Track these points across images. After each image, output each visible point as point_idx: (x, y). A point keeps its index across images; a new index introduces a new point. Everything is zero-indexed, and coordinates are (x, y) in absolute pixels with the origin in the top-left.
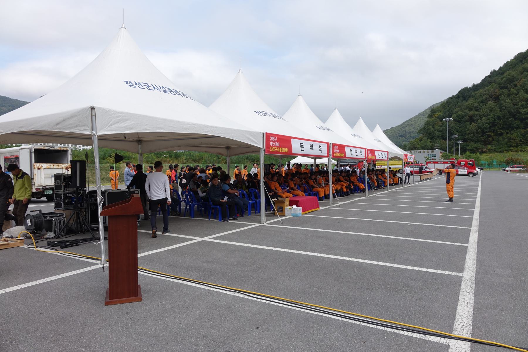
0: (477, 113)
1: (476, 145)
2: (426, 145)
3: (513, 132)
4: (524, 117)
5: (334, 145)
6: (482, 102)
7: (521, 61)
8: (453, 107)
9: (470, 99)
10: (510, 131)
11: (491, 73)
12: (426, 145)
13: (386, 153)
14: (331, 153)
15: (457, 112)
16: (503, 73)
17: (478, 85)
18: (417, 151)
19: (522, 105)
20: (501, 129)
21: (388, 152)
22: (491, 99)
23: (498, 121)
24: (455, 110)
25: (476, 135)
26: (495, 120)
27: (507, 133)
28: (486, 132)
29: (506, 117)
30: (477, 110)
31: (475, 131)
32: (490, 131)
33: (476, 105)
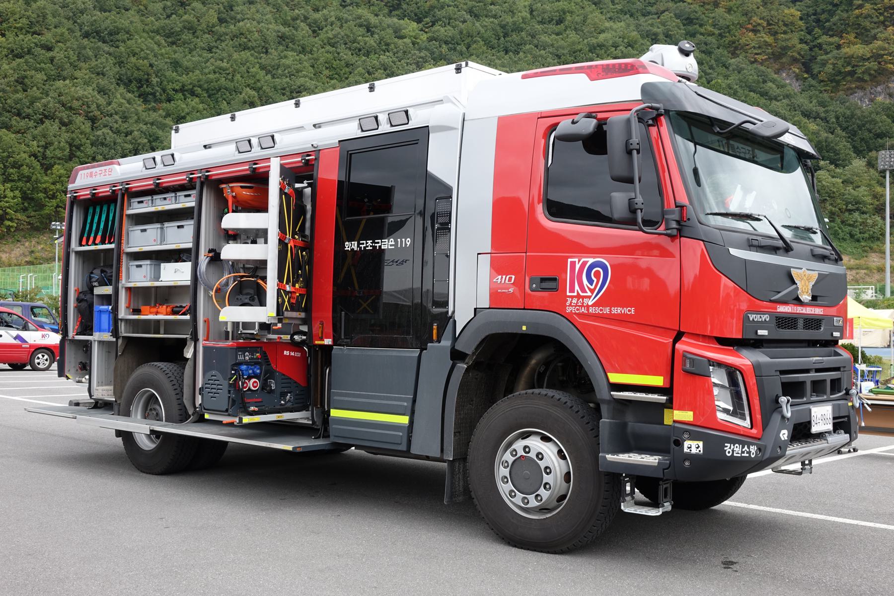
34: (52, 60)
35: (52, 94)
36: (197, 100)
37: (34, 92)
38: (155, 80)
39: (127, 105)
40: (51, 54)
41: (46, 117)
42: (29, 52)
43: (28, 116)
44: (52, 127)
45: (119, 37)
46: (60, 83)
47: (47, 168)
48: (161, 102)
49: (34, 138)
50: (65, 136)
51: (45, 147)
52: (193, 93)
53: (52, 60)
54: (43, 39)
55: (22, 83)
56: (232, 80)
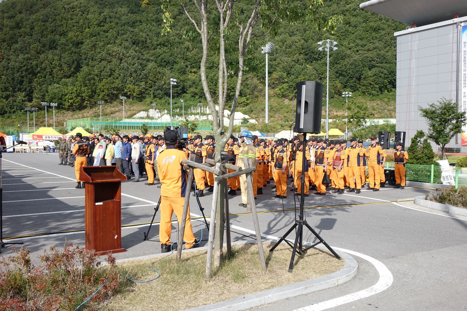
34: (107, 37)
35: (105, 50)
36: (165, 48)
37: (98, 50)
38: (148, 41)
40: (107, 34)
41: (103, 60)
42: (99, 34)
44: (104, 63)
45: (137, 24)
46: (109, 46)
47: (101, 80)
50: (109, 67)
51: (101, 72)
52: (164, 45)
53: (107, 37)
54: (104, 28)
56: (181, 39)
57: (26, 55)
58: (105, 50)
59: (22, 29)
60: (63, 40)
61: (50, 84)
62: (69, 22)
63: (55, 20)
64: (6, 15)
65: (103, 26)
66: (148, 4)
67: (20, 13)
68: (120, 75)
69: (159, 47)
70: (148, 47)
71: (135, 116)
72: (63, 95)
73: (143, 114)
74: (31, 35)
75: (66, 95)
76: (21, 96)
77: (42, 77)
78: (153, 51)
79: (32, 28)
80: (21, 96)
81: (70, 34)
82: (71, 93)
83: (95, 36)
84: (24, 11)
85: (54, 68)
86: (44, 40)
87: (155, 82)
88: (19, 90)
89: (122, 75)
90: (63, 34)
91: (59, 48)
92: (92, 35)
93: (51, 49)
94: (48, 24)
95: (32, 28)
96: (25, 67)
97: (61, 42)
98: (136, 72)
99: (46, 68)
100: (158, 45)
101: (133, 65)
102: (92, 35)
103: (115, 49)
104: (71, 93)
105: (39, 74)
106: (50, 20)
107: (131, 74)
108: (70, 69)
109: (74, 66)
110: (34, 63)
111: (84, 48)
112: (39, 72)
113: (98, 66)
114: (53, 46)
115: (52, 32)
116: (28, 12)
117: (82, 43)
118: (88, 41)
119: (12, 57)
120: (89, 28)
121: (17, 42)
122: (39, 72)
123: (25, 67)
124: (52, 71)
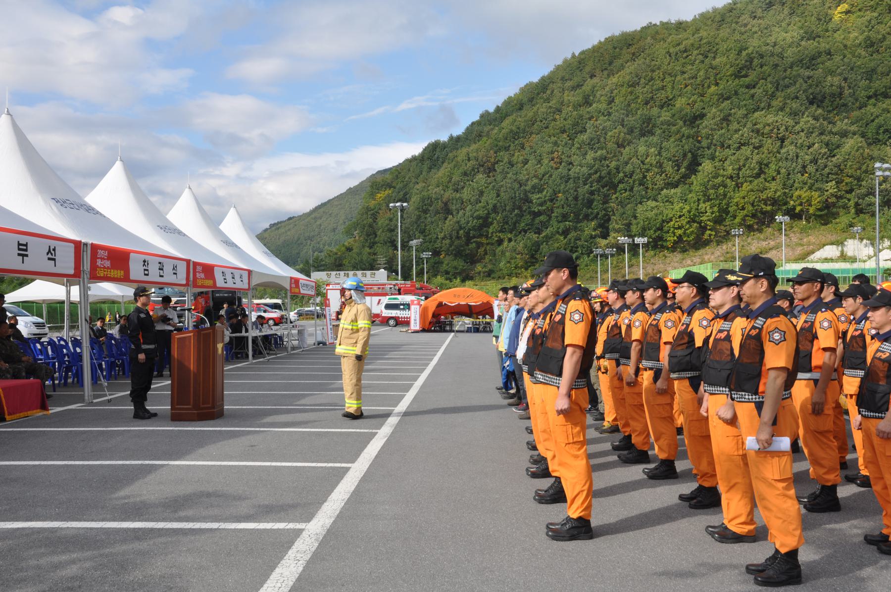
0: (458, 195)
1: (455, 263)
2: (361, 261)
3: (519, 238)
4: (536, 210)
5: (95, 248)
6: (465, 174)
7: (531, 100)
8: (413, 180)
9: (445, 164)
10: (516, 236)
11: (482, 116)
12: (361, 261)
13: (245, 274)
14: (86, 265)
15: (421, 192)
16: (502, 119)
17: (458, 138)
18: (342, 273)
19: (534, 187)
20: (500, 231)
21: (250, 272)
22: (482, 169)
23: (493, 215)
24: (417, 186)
25: (457, 242)
26: (489, 213)
27: (510, 240)
28: (474, 237)
29: (508, 208)
30: (457, 191)
31: (454, 233)
32: (481, 236)
33: (455, 178)
34: (753, 96)
35: (749, 125)
37: (734, 126)
38: (847, 92)
39: (814, 122)
40: (752, 91)
41: (742, 145)
42: (736, 93)
43: (729, 147)
44: (746, 151)
45: (819, 60)
46: (757, 114)
47: (738, 186)
48: (853, 110)
49: (731, 164)
50: (756, 158)
51: (740, 169)
53: (753, 96)
54: (747, 80)
55: (726, 119)
57: (599, 153)
58: (749, 125)
59: (594, 105)
60: (665, 116)
61: (641, 203)
62: (678, 78)
63: (652, 79)
64: (568, 84)
65: (746, 76)
66: (847, 12)
67: (592, 76)
68: (779, 173)
69: (873, 101)
70: (845, 105)
71: (812, 257)
72: (663, 221)
73: (831, 251)
74: (609, 114)
75: (671, 220)
76: (589, 228)
77: (626, 190)
78: (856, 113)
79: (611, 101)
80: (589, 228)
81: (680, 103)
82: (680, 217)
83: (728, 98)
84: (598, 72)
85: (648, 170)
86: (631, 120)
87: (859, 179)
88: (587, 217)
89: (783, 171)
90: (667, 104)
91: (659, 132)
92: (723, 98)
93: (643, 135)
94: (639, 89)
95: (611, 101)
96: (598, 174)
97: (661, 119)
98: (815, 161)
99: (633, 172)
100: (869, 97)
101: (809, 147)
102: (723, 98)
103: (770, 119)
104: (680, 217)
105: (621, 186)
106: (643, 81)
107: (804, 167)
108: (678, 170)
109: (685, 164)
110: (613, 164)
111: (706, 124)
112: (620, 182)
113: (733, 158)
114: (646, 129)
115: (647, 103)
116: (606, 73)
117: (702, 116)
118: (714, 110)
119: (576, 159)
120: (717, 84)
121: (584, 130)
122: (620, 182)
123: (598, 174)
124: (645, 177)
